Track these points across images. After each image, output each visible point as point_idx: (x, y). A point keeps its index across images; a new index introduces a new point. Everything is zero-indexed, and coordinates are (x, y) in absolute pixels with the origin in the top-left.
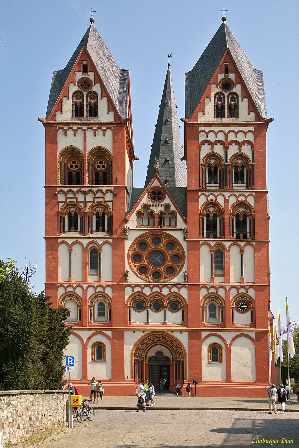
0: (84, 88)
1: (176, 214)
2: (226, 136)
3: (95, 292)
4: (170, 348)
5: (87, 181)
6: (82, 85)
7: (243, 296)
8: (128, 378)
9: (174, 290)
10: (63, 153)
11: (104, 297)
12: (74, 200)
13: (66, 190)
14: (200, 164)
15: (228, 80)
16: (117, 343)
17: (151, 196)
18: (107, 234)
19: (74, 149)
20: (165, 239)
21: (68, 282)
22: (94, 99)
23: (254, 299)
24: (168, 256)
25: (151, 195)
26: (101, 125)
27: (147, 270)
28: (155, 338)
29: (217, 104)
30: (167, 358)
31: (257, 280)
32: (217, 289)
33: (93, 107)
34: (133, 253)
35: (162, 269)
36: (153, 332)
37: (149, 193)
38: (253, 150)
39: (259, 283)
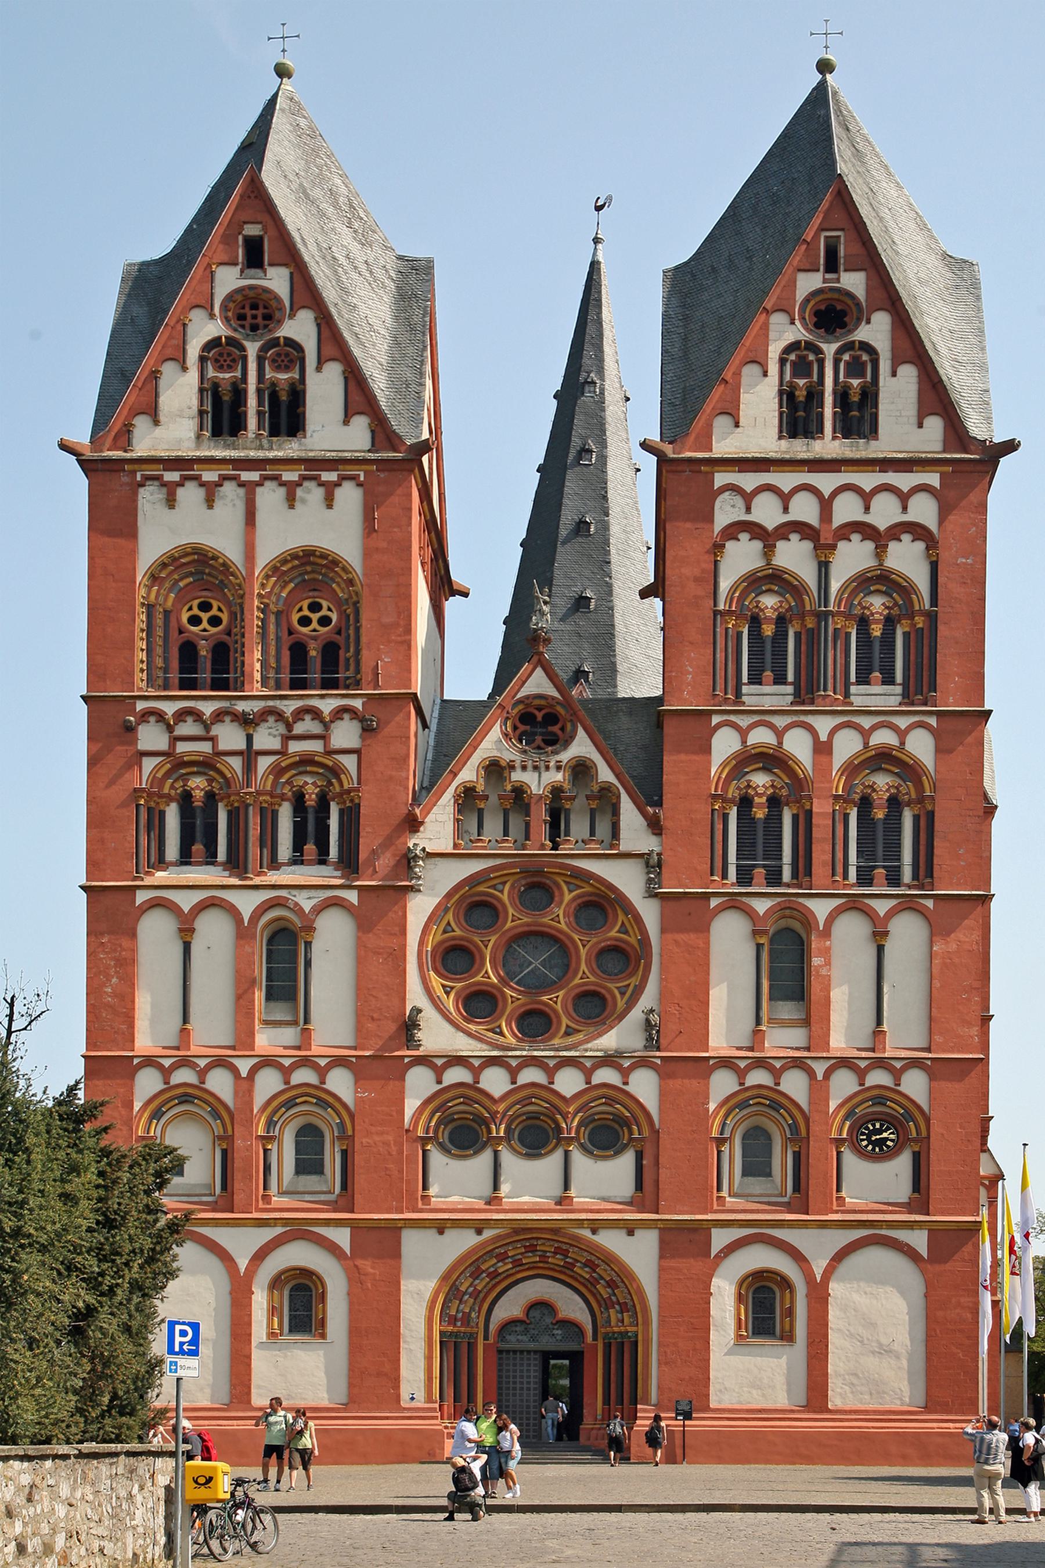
0: (247, 326)
1: (619, 797)
2: (826, 505)
3: (283, 1087)
4: (584, 1289)
5: (258, 676)
6: (241, 317)
7: (880, 1096)
8: (413, 1399)
10: (160, 571)
11: (322, 1103)
12: (206, 747)
13: (170, 708)
14: (716, 613)
15: (836, 296)
16: (372, 1271)
18: (338, 873)
19: (206, 556)
20: (570, 891)
21: (178, 1048)
22: (287, 369)
23: (926, 1108)
24: (583, 952)
25: (515, 728)
26: (314, 465)
27: (496, 1006)
28: (526, 1252)
29: (793, 386)
30: (571, 1326)
31: (937, 1038)
32: (777, 1074)
33: (284, 398)
35: (557, 1000)
36: (516, 1231)
37: (507, 718)
38: (934, 559)
39: (944, 1051)
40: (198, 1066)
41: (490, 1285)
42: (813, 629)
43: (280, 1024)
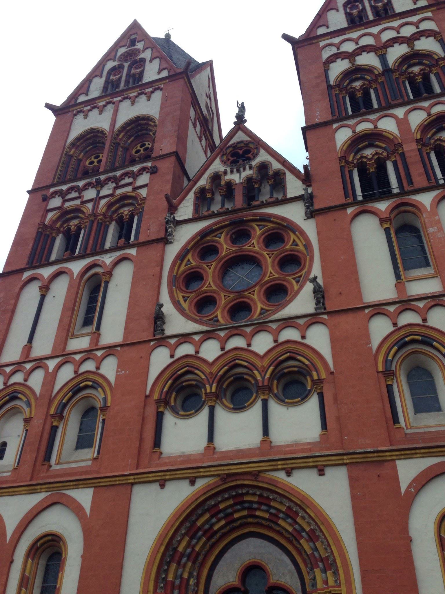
11: (95, 386)
12: (78, 202)
17: (230, 161)
20: (260, 230)
24: (269, 260)
25: (229, 160)
34: (184, 272)
42: (383, 82)
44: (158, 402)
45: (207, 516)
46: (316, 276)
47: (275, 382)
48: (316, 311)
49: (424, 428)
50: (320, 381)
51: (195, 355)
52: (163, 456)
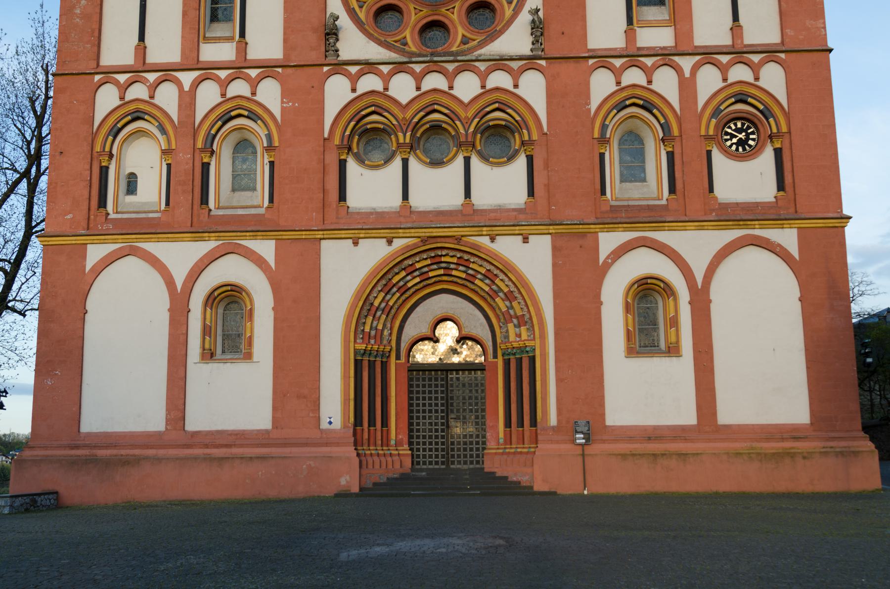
3: (220, 100)
9: (500, 79)
11: (253, 116)
36: (425, 240)
40: (148, 80)
41: (401, 301)
43: (219, 40)
44: (339, 147)
45: (403, 274)
46: (538, 8)
47: (479, 136)
48: (532, 52)
49: (628, 200)
50: (531, 142)
51: (383, 93)
52: (350, 210)
